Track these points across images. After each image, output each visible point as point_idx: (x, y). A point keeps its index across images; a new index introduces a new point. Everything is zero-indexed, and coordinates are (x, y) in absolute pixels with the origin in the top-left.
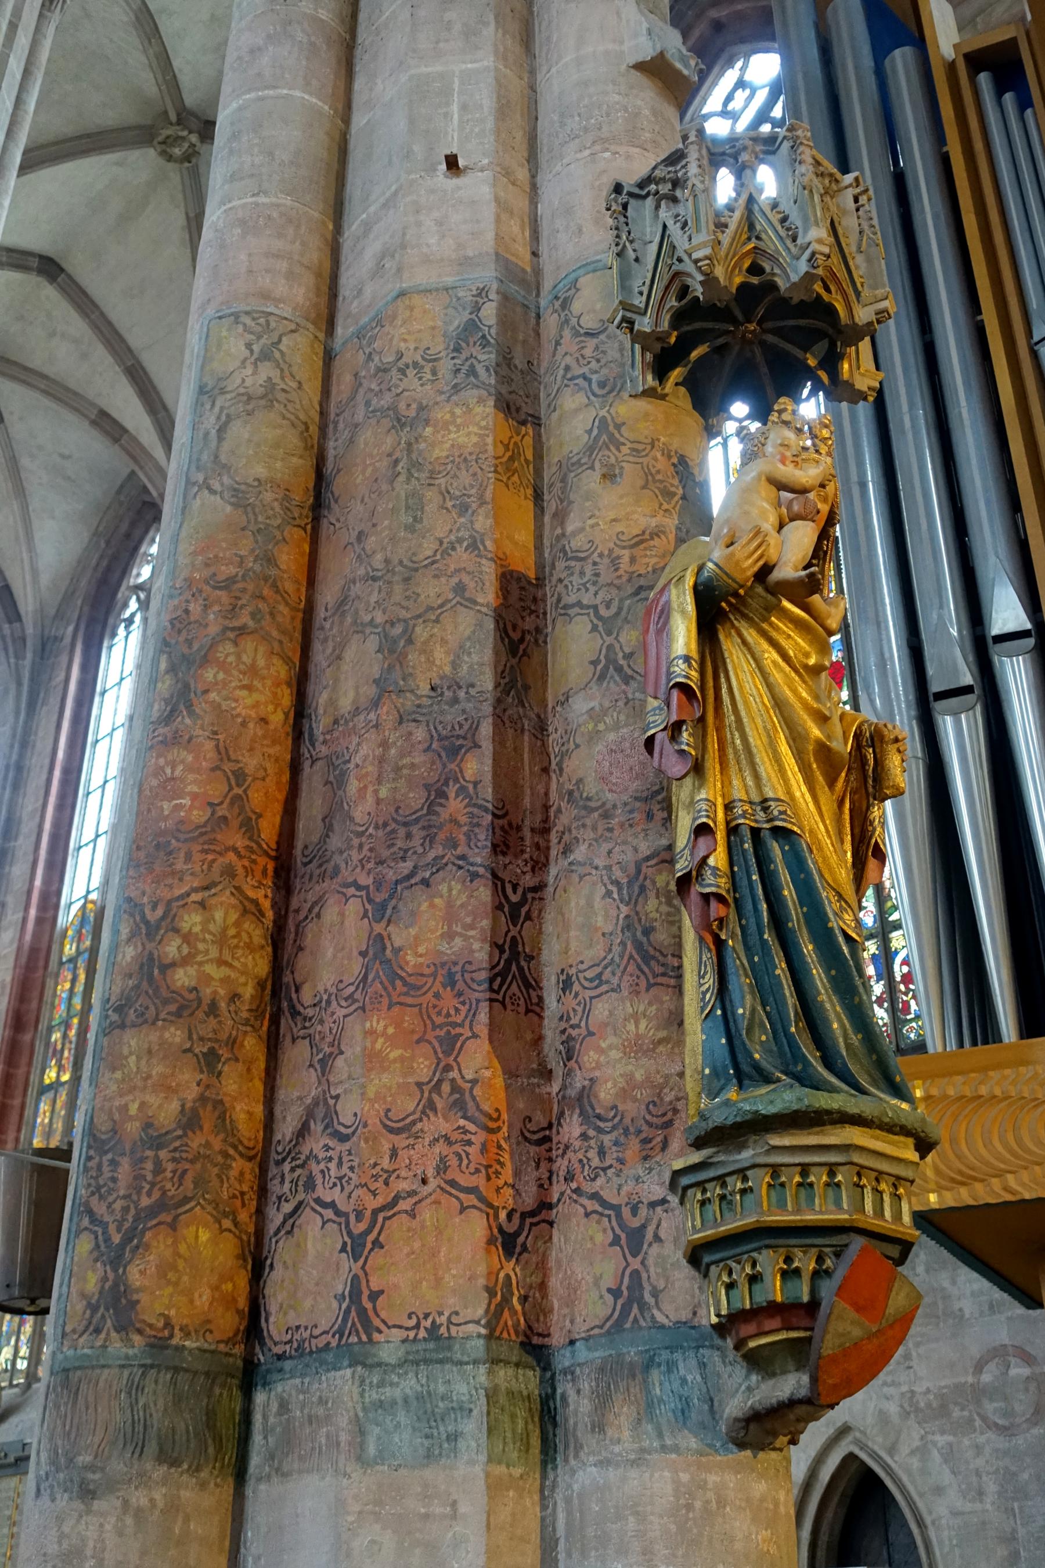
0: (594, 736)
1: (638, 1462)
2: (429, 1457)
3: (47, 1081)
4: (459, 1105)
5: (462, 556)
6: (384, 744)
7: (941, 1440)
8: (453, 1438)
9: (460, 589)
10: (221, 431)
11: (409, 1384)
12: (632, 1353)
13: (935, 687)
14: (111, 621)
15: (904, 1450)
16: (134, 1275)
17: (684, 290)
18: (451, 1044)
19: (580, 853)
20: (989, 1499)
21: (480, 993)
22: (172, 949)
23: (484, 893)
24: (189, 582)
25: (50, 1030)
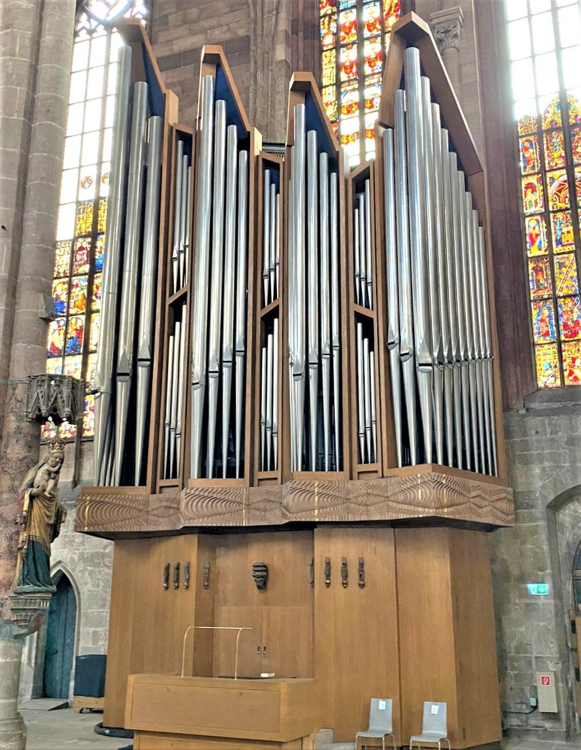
0: (7, 505)
17: (40, 410)
20: (101, 587)
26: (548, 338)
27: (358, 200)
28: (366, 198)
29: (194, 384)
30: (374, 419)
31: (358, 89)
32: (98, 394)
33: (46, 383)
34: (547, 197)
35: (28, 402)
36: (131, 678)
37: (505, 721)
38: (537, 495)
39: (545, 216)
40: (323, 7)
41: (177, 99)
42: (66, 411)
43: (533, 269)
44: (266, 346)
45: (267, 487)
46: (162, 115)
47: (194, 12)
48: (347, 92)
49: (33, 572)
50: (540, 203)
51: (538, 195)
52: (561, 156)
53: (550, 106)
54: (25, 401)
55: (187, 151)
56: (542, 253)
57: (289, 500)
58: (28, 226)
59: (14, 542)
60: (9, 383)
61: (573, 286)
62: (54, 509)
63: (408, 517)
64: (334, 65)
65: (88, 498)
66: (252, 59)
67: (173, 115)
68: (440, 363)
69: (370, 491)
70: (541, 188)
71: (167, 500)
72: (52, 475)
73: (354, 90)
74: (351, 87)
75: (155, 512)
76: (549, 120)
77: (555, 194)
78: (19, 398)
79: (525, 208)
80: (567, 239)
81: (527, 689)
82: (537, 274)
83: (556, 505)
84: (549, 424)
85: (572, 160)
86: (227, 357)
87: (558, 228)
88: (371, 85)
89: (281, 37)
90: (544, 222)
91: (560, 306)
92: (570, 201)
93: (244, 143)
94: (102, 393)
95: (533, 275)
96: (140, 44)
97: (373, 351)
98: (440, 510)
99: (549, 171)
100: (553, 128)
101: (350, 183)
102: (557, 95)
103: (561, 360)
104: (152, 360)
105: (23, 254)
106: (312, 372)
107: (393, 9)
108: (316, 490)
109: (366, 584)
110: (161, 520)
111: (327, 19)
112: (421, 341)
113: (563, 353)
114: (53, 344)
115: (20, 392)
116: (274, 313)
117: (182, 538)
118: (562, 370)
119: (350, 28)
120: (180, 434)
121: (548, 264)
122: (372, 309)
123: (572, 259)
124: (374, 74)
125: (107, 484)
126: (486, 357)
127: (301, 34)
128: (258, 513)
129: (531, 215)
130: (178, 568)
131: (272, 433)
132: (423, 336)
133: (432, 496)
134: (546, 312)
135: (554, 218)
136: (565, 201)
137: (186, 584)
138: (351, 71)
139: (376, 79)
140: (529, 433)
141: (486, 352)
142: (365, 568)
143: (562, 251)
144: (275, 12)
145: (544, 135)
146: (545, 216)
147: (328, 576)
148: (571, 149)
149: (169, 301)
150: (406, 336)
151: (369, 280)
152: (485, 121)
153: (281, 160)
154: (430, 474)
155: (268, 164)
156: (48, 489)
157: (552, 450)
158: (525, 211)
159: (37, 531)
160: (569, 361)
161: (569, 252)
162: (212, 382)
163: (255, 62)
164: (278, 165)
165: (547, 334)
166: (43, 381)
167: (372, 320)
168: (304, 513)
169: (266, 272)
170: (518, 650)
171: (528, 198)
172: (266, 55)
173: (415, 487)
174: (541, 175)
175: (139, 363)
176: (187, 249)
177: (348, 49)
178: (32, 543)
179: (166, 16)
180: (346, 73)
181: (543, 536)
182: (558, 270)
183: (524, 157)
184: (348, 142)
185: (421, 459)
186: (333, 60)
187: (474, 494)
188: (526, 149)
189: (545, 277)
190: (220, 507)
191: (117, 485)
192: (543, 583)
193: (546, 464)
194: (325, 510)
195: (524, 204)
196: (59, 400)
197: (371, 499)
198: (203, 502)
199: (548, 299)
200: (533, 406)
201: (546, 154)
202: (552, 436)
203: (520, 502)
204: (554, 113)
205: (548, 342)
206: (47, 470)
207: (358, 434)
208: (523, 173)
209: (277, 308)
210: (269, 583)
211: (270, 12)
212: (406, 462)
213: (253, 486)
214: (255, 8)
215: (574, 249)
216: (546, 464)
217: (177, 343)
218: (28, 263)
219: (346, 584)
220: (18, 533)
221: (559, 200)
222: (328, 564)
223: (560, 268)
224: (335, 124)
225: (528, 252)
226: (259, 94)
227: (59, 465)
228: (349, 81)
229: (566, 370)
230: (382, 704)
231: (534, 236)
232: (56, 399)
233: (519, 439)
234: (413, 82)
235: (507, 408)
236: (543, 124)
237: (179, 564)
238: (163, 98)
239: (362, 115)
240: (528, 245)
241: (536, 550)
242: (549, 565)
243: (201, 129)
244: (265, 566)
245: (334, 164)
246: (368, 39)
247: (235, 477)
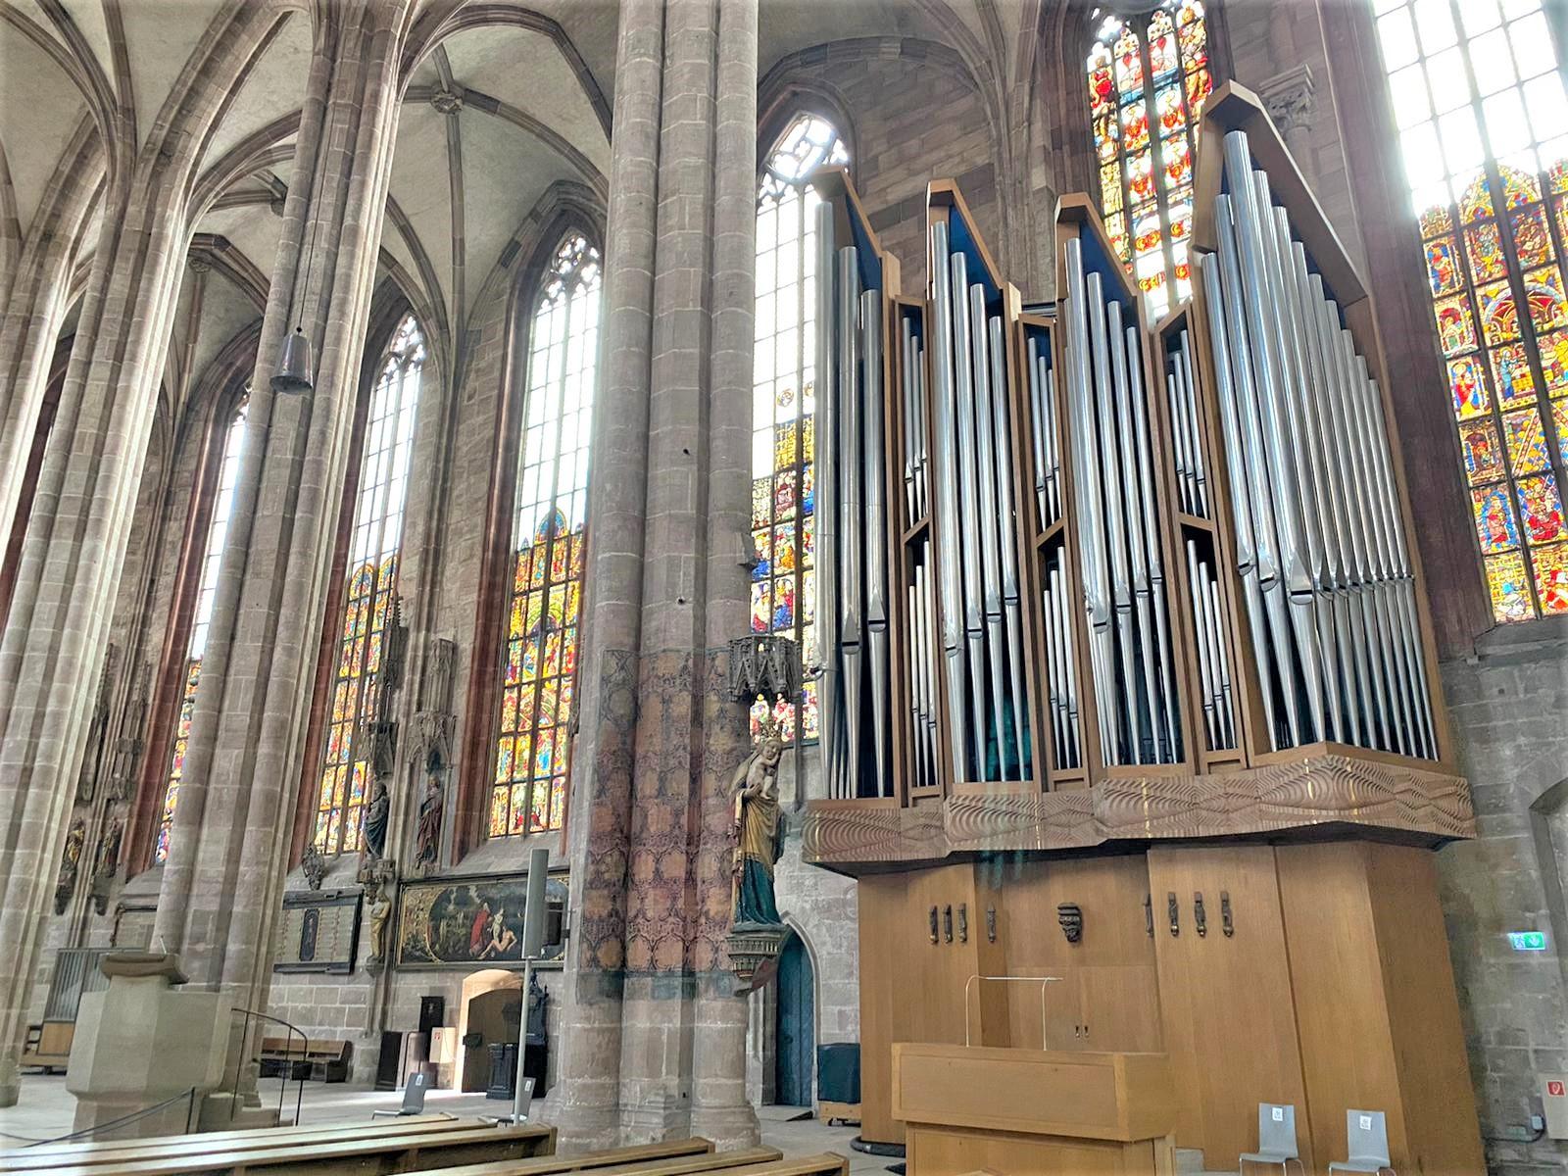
0: (714, 813)
1: (715, 999)
2: (669, 998)
3: (341, 675)
4: (677, 915)
5: (681, 752)
6: (659, 811)
7: (827, 922)
8: (675, 994)
9: (680, 763)
10: (610, 696)
11: (665, 982)
12: (715, 976)
13: (844, 640)
14: (376, 374)
15: (811, 925)
16: (599, 955)
17: (747, 685)
18: (675, 899)
19: (709, 846)
21: (682, 886)
22: (603, 868)
23: (684, 857)
24: (603, 751)
25: (343, 642)
26: (1504, 544)
27: (1173, 362)
28: (1184, 359)
29: (948, 649)
30: (1226, 682)
31: (1158, 211)
32: (819, 673)
33: (753, 647)
34: (1481, 327)
35: (731, 675)
36: (896, 1048)
37: (1490, 1156)
38: (1511, 791)
39: (1481, 355)
40: (1096, 106)
41: (897, 263)
42: (780, 684)
43: (1468, 438)
44: (1049, 588)
45: (1069, 790)
46: (879, 288)
47: (913, 145)
48: (1141, 218)
49: (753, 902)
50: (1470, 337)
51: (1464, 325)
52: (1497, 261)
53: (1471, 187)
54: (728, 675)
55: (916, 330)
56: (1480, 412)
57: (1104, 808)
58: (717, 447)
59: (726, 863)
60: (707, 652)
61: (1539, 459)
62: (774, 817)
63: (1295, 825)
64: (1118, 184)
66: (998, 195)
67: (893, 286)
68: (1326, 589)
69: (1230, 790)
70: (1469, 313)
71: (927, 815)
72: (769, 770)
73: (1151, 214)
74: (1147, 210)
75: (911, 833)
76: (1471, 209)
77: (1493, 319)
78: (720, 670)
79: (1443, 349)
80: (1521, 387)
81: (1525, 1101)
82: (1476, 447)
83: (1546, 806)
84: (1520, 676)
85: (1518, 264)
86: (993, 608)
87: (1503, 371)
88: (1176, 203)
89: (1038, 156)
90: (1478, 365)
91: (1521, 492)
92: (1520, 326)
93: (996, 306)
94: (824, 671)
95: (1468, 449)
96: (843, 196)
97: (1216, 580)
98: (1347, 812)
99: (1479, 286)
100: (1480, 219)
101: (1157, 339)
102: (1482, 169)
103: (1532, 577)
104: (887, 621)
105: (712, 484)
106: (1123, 619)
107: (1201, 90)
108: (1145, 792)
109: (1235, 930)
110: (919, 844)
111: (1102, 120)
112: (1291, 558)
113: (1534, 565)
114: (756, 618)
115: (721, 663)
116: (1058, 539)
117: (951, 870)
118: (1535, 593)
119: (1139, 127)
120: (935, 722)
121: (1493, 428)
122: (1209, 518)
123: (1533, 415)
124: (1181, 186)
125: (841, 796)
126: (1401, 577)
127: (1066, 148)
128: (1059, 830)
129: (1456, 357)
130: (949, 913)
131: (1069, 714)
132: (1293, 550)
133: (1331, 791)
134: (1497, 504)
135: (1495, 357)
136: (1512, 328)
137: (962, 934)
138: (1145, 188)
139: (1183, 193)
140: (1487, 693)
141: (1400, 568)
142: (1232, 907)
143: (1516, 406)
144: (1026, 124)
145: (1466, 232)
146: (1481, 355)
147: (1174, 920)
148: (1514, 246)
149: (905, 538)
150: (1266, 553)
151: (1200, 476)
152: (1362, 225)
153: (1050, 323)
154: (1324, 757)
155: (1031, 330)
156: (766, 787)
157: (1533, 719)
158: (1445, 353)
159: (754, 846)
160: (1545, 577)
161: (1529, 406)
162: (974, 645)
163: (1003, 198)
164: (1047, 330)
165: (1502, 538)
166: (749, 645)
167: (1209, 534)
168: (1129, 827)
169: (1040, 482)
170: (1502, 1038)
171: (1446, 333)
172: (1018, 185)
173: (1303, 778)
175: (870, 627)
176: (925, 465)
177: (1138, 157)
178: (749, 862)
179: (876, 158)
180: (1139, 192)
181: (1529, 857)
182: (1511, 437)
184: (1150, 287)
185: (1308, 736)
186: (1117, 176)
187: (1401, 787)
188: (1437, 259)
189: (1490, 449)
191: (854, 797)
192: (1534, 930)
193: (1522, 740)
194: (1160, 821)
196: (770, 669)
197: (1234, 802)
199: (1499, 482)
200: (1489, 650)
201: (1471, 261)
202: (1529, 696)
203: (1480, 801)
204: (1479, 198)
205: (1506, 549)
206: (763, 764)
207: (1203, 706)
208: (1435, 296)
209: (1061, 532)
210: (1085, 933)
211: (1018, 125)
212: (1284, 742)
213: (1047, 791)
214: (997, 125)
215: (1536, 400)
216: (1522, 740)
217: (920, 597)
218: (719, 497)
219: (1204, 931)
220: (730, 852)
221: (1501, 327)
222: (1173, 902)
223: (1515, 432)
224: (1128, 266)
225: (1457, 414)
226: (1012, 241)
227: (777, 756)
228: (1143, 202)
229: (1542, 592)
230: (1277, 1113)
231: (1464, 389)
232: (766, 668)
233: (1470, 705)
234: (1241, 184)
235: (1445, 658)
236: (1461, 217)
237: (949, 908)
238: (879, 264)
239: (1167, 250)
240: (1455, 403)
241: (1519, 878)
242: (1544, 902)
243: (934, 297)
244: (1076, 908)
245: (1130, 317)
246: (1166, 138)
247: (1020, 779)
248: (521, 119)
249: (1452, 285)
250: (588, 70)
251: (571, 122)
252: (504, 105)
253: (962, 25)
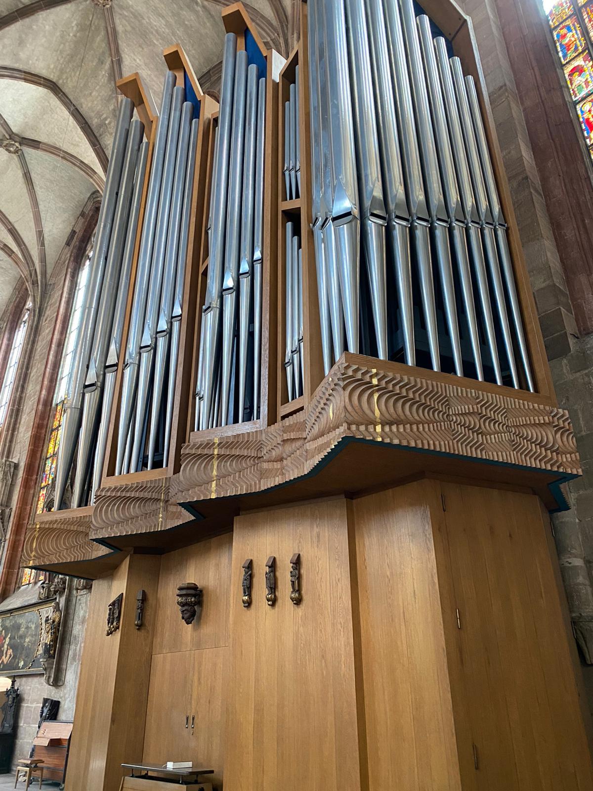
65: (38, 526)
79: (573, 97)
109: (305, 597)
129: (583, 99)
145: (583, 10)
171: (574, 85)
174: (587, 51)
183: (561, 45)
188: (564, 36)
190: (134, 510)
195: (572, 92)
198: (115, 504)
208: (564, 62)
240: (585, 133)
248: (53, 150)
249: (576, 49)
250: (77, 109)
251: (78, 145)
252: (44, 144)
253: (263, 17)
